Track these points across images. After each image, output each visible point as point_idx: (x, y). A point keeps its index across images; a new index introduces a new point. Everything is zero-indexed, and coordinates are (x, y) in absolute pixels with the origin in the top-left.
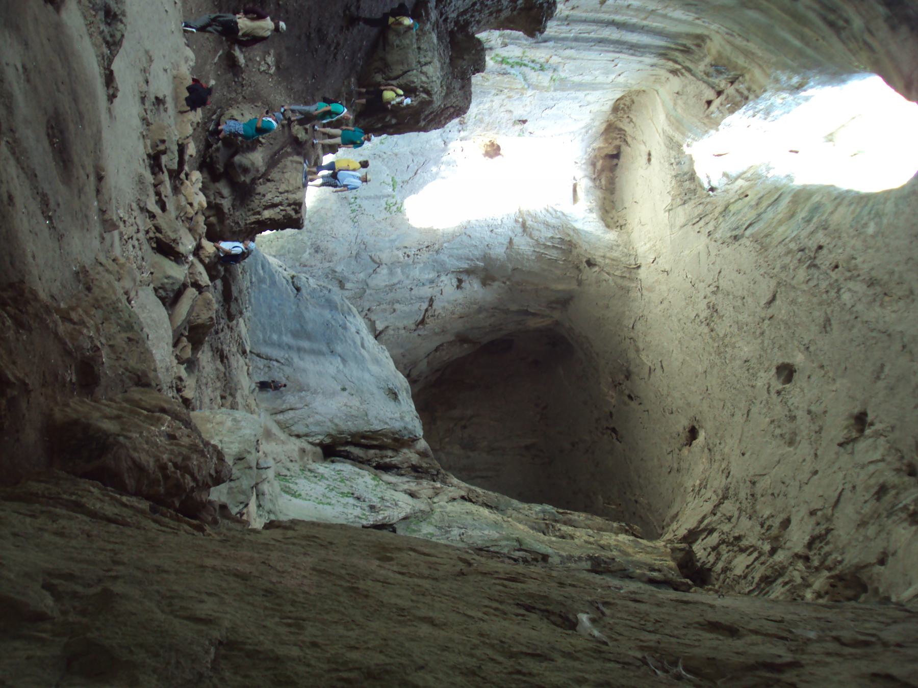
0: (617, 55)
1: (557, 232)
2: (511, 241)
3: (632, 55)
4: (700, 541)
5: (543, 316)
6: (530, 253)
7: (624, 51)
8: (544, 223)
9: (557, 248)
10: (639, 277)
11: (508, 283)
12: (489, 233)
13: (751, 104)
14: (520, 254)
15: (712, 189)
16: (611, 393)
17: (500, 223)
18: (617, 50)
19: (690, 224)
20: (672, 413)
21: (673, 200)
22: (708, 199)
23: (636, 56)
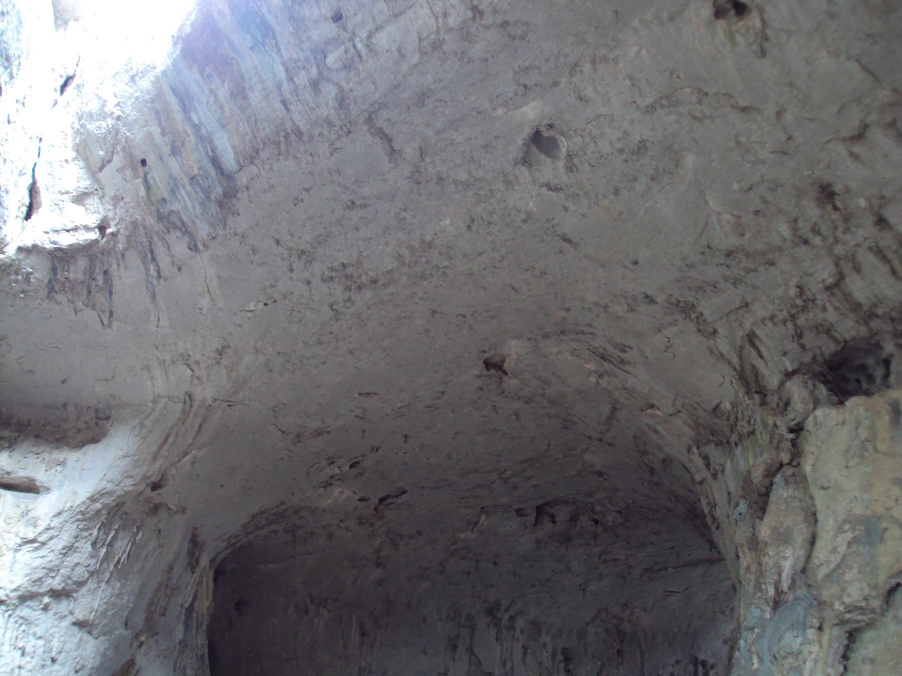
1: (86, 534)
2: (80, 624)
4: (760, 364)
5: (200, 583)
6: (110, 590)
8: (65, 554)
9: (114, 538)
10: (209, 402)
11: (143, 638)
12: (56, 667)
14: (106, 611)
15: (102, 228)
16: (336, 494)
17: (41, 642)
19: (155, 282)
20: (443, 393)
21: (94, 307)
22: (121, 238)
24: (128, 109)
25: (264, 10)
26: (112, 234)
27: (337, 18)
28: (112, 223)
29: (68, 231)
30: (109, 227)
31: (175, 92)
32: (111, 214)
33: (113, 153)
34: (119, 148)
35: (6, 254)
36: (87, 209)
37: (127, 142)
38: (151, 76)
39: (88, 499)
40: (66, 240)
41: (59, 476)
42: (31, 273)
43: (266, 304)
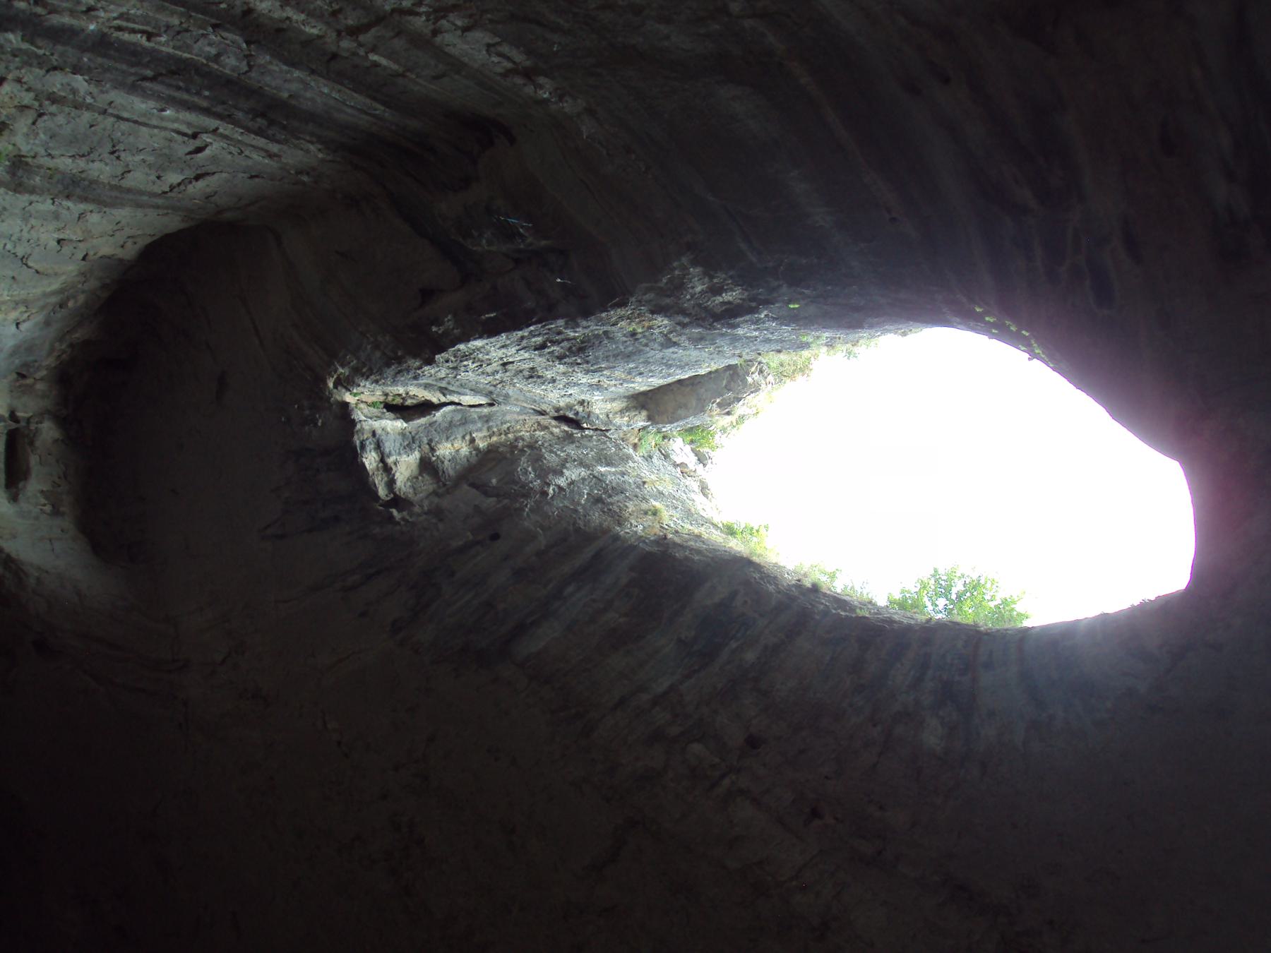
0: (212, 123)
3: (259, 133)
7: (240, 115)
13: (561, 322)
15: (397, 501)
18: (219, 109)
23: (272, 139)
24: (558, 503)
25: (734, 645)
26: (391, 517)
27: (753, 743)
28: (405, 513)
29: (382, 460)
30: (399, 512)
31: (598, 556)
32: (417, 509)
33: (497, 496)
34: (506, 501)
35: (335, 391)
36: (417, 478)
37: (516, 510)
38: (608, 522)
39: (8, 556)
40: (370, 460)
41: (36, 510)
42: (316, 424)
43: (339, 743)
